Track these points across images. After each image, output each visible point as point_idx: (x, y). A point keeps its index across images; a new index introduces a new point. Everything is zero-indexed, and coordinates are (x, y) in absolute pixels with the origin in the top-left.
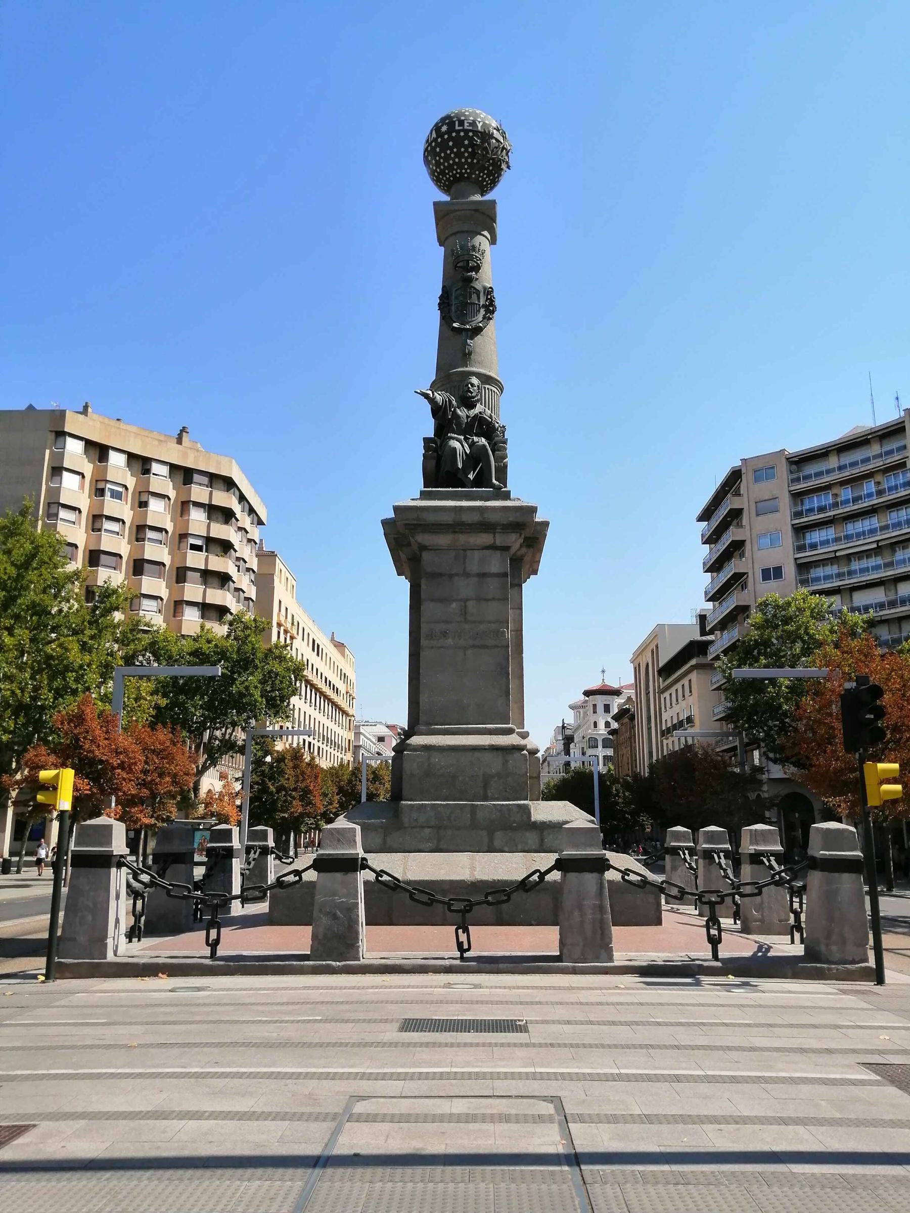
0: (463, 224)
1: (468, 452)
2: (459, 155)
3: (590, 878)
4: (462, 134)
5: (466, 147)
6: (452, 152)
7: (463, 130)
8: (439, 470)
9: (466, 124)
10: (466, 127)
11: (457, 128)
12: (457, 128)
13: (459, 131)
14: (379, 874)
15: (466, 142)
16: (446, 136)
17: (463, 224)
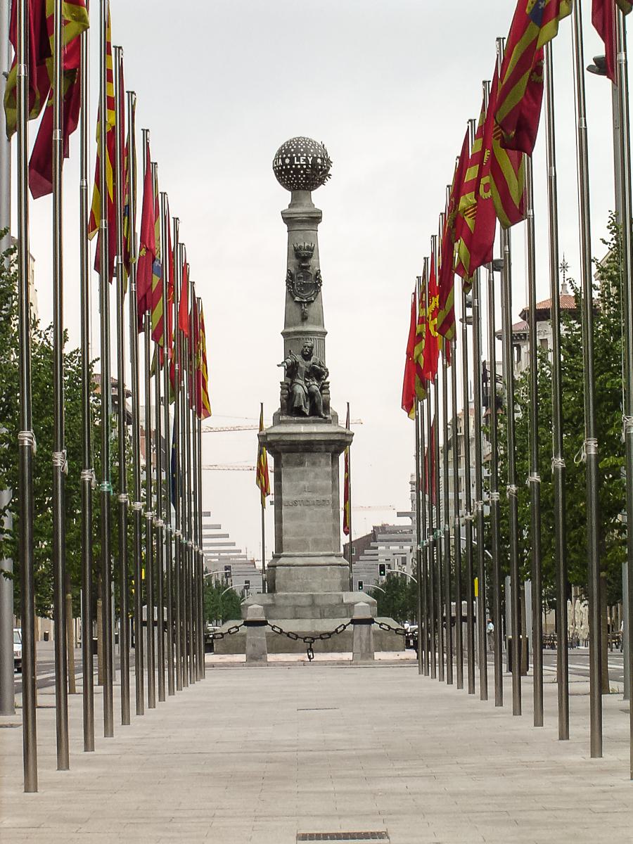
0: (302, 222)
1: (307, 392)
2: (297, 178)
3: (365, 627)
4: (299, 167)
5: (302, 175)
6: (292, 177)
7: (300, 164)
8: (290, 407)
9: (301, 160)
10: (301, 163)
11: (296, 163)
12: (296, 163)
13: (297, 165)
14: (273, 627)
15: (302, 172)
16: (289, 167)
17: (302, 222)
